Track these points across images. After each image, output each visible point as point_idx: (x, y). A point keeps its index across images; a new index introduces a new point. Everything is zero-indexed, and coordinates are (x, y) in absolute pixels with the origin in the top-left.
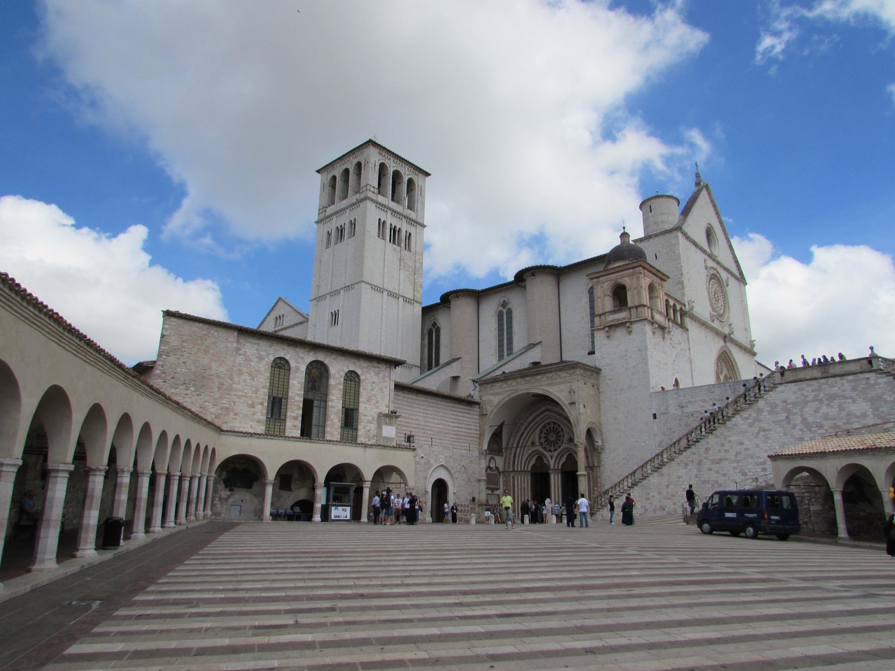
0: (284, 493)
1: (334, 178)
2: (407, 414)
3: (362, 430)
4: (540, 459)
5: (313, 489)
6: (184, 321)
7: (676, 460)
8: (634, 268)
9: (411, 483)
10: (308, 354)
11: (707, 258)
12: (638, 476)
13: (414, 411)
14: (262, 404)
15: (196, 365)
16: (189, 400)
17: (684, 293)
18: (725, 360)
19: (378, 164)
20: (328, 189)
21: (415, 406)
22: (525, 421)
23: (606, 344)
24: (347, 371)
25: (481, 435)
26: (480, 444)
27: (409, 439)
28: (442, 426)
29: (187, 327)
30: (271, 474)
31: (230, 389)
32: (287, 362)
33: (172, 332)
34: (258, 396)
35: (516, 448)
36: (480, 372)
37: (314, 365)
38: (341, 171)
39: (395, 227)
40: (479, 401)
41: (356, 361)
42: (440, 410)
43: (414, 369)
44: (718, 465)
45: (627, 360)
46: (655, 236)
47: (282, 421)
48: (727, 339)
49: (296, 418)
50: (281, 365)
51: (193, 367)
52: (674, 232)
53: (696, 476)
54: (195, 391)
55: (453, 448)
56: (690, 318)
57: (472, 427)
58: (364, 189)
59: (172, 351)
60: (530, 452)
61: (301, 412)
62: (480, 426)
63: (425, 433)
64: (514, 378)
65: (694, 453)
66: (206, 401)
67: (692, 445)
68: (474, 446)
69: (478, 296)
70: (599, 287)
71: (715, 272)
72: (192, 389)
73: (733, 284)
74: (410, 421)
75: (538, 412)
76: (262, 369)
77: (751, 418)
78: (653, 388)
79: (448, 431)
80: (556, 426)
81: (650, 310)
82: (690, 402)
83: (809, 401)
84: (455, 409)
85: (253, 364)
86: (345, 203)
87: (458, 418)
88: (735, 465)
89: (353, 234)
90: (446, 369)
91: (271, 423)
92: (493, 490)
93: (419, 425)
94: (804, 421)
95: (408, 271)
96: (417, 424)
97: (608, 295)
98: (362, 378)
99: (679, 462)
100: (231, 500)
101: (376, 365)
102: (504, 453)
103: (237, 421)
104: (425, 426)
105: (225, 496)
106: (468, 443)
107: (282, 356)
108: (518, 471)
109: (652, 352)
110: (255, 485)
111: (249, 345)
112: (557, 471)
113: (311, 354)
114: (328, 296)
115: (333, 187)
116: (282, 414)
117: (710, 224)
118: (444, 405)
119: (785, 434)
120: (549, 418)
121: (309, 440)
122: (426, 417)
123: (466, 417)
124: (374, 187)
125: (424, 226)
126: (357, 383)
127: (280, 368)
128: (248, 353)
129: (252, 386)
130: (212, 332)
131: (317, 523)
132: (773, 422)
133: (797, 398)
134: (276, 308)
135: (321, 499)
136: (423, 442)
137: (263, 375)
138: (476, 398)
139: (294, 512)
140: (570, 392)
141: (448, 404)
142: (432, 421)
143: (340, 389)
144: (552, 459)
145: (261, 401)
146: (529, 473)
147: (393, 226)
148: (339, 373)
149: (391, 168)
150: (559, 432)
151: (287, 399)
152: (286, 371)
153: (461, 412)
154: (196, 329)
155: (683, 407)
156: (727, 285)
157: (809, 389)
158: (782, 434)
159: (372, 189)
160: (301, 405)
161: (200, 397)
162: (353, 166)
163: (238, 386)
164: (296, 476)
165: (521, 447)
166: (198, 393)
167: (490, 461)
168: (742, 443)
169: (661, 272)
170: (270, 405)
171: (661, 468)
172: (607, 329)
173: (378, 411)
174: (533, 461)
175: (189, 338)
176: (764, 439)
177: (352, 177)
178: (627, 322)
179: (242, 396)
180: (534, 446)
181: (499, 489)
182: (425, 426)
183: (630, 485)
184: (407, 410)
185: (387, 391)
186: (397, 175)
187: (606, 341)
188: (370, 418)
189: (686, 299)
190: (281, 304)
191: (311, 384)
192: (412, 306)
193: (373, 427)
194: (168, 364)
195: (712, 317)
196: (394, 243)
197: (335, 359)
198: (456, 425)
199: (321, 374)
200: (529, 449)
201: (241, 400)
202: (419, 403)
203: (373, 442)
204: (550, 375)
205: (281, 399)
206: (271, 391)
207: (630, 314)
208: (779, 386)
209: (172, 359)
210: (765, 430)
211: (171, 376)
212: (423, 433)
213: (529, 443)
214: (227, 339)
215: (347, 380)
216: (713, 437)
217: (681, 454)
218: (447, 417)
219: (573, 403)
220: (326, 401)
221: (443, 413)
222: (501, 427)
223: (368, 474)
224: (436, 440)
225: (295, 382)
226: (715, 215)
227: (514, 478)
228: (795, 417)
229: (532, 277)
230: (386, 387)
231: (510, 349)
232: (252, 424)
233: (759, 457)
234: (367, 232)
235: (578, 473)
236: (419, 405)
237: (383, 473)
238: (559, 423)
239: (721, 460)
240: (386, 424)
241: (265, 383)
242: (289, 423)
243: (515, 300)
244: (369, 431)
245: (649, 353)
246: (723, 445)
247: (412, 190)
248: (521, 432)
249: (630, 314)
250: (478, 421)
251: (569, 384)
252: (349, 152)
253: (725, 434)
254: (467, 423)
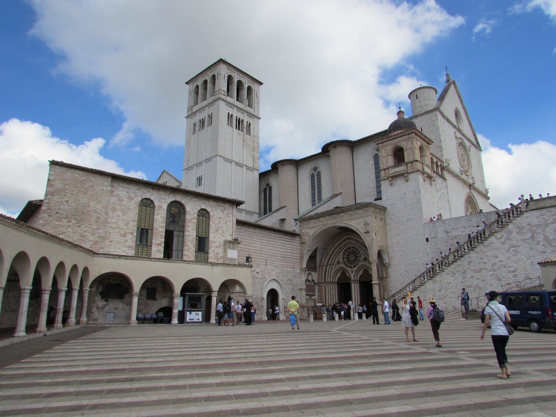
0: (150, 302)
1: (197, 87)
2: (248, 242)
3: (211, 253)
4: (344, 273)
5: (172, 298)
6: (67, 169)
7: (446, 271)
8: (409, 134)
9: (249, 292)
10: (169, 196)
11: (456, 131)
12: (417, 283)
13: (253, 241)
14: (132, 233)
15: (77, 203)
16: (71, 230)
17: (442, 154)
18: (470, 202)
19: (226, 76)
20: (193, 94)
21: (254, 237)
22: (333, 246)
23: (389, 190)
24: (199, 209)
25: (302, 257)
26: (301, 264)
27: (248, 259)
28: (273, 251)
29: (69, 173)
30: (137, 287)
31: (106, 222)
32: (152, 202)
33: (57, 177)
34: (129, 227)
35: (327, 266)
36: (300, 214)
37: (174, 204)
38: (202, 82)
39: (239, 118)
40: (299, 233)
41: (206, 201)
42: (271, 240)
43: (254, 215)
44: (478, 274)
45: (405, 200)
46: (420, 115)
47: (148, 247)
48: (471, 187)
49: (159, 245)
50: (147, 204)
51: (74, 205)
52: (434, 111)
53: (462, 282)
54: (76, 224)
55: (282, 267)
56: (447, 171)
57: (295, 252)
58: (218, 93)
59: (57, 192)
60: (336, 268)
61: (163, 240)
62: (300, 251)
63: (261, 256)
64: (324, 216)
65: (459, 265)
66: (84, 232)
67: (458, 259)
68: (296, 265)
69: (297, 164)
70: (383, 150)
71: (461, 141)
72: (74, 222)
73: (473, 149)
74: (250, 248)
75: (341, 240)
76: (132, 207)
77: (503, 238)
78: (425, 220)
79: (278, 255)
80: (355, 250)
81: (421, 164)
82: (454, 228)
83: (550, 224)
84: (283, 239)
85: (124, 203)
86: (205, 103)
87: (284, 245)
88: (492, 273)
89: (210, 123)
90: (276, 214)
91: (140, 248)
92: (310, 296)
93: (257, 250)
94: (546, 238)
95: (249, 148)
96: (255, 250)
97: (390, 155)
98: (211, 214)
99: (448, 272)
100: (106, 309)
101: (222, 205)
102: (318, 270)
103: (112, 247)
104: (261, 251)
105: (102, 306)
106: (293, 263)
107: (148, 197)
108: (328, 282)
109: (424, 194)
110: (126, 296)
111: (121, 188)
112: (356, 282)
113: (171, 196)
114: (195, 167)
115: (197, 93)
116: (149, 241)
117: (457, 108)
118: (274, 236)
119: (531, 249)
120: (349, 244)
121: (167, 261)
122: (261, 245)
123: (290, 245)
124: (224, 91)
125: (260, 119)
126: (207, 218)
127: (146, 206)
128: (120, 195)
129: (124, 220)
130: (90, 178)
131: (175, 325)
132: (521, 240)
133: (539, 221)
134: (161, 177)
135: (177, 306)
136: (259, 263)
137: (133, 211)
138: (298, 231)
139: (158, 317)
140: (365, 224)
141: (278, 236)
142: (266, 247)
143: (194, 223)
144: (352, 273)
145: (131, 231)
146: (336, 284)
147: (238, 118)
148: (193, 211)
149: (236, 79)
150: (357, 254)
151: (152, 230)
152: (151, 209)
153: (287, 241)
154: (77, 176)
155: (448, 232)
156: (470, 151)
157: (549, 214)
158: (528, 249)
159: (223, 93)
160: (164, 235)
161: (80, 228)
162: (210, 78)
163: (113, 220)
164: (159, 289)
165: (330, 265)
166: (78, 225)
167: (308, 276)
168: (497, 257)
169: (427, 138)
170: (139, 235)
171: (435, 277)
172: (390, 179)
173: (224, 239)
174: (339, 275)
175: (71, 182)
176: (514, 253)
177: (209, 85)
178: (405, 173)
179: (116, 228)
180: (339, 264)
181: (315, 295)
182: (261, 251)
183: (411, 290)
184: (247, 240)
185: (230, 224)
186: (240, 83)
187: (390, 188)
188: (218, 244)
189: (444, 158)
190: (165, 174)
191: (171, 219)
192: (252, 172)
193: (220, 251)
194: (53, 202)
195: (461, 171)
196: (239, 129)
197: (190, 200)
198: (284, 250)
199: (180, 212)
200: (335, 267)
201: (115, 231)
202: (257, 234)
203: (221, 262)
204: (350, 213)
205: (147, 230)
206: (140, 224)
207: (407, 168)
208: (525, 213)
209: (56, 198)
210: (514, 246)
211: (56, 211)
212: (259, 256)
213: (336, 262)
214: (102, 184)
215: (199, 216)
216: (474, 253)
217: (450, 266)
218: (277, 245)
219: (367, 232)
220: (183, 232)
221: (274, 242)
222: (315, 251)
223: (215, 286)
224: (269, 261)
225: (159, 217)
226: (460, 103)
227: (325, 287)
228: (539, 236)
229: (334, 149)
230: (230, 221)
231: (320, 199)
232: (124, 249)
233: (511, 267)
234: (220, 122)
235: (373, 282)
236: (256, 236)
237: (227, 285)
238: (357, 247)
239: (481, 270)
240: (230, 248)
241: (135, 218)
242: (154, 248)
243: (322, 165)
244: (217, 254)
245: (422, 195)
246: (482, 258)
247: (250, 94)
248: (329, 255)
249: (407, 168)
250: (299, 247)
251: (364, 219)
252: (207, 68)
253: (483, 250)
254: (290, 249)
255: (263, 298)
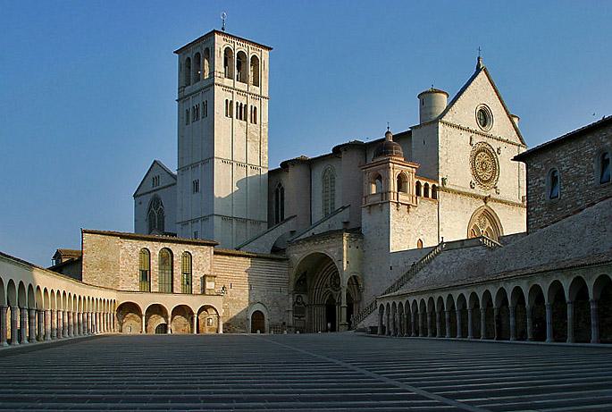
1: (189, 59)
4: (331, 296)
43: (262, 225)
69: (308, 164)
115: (190, 68)
159: (219, 75)
196: (241, 119)
223: (195, 311)
243: (334, 164)
255: (248, 319)
